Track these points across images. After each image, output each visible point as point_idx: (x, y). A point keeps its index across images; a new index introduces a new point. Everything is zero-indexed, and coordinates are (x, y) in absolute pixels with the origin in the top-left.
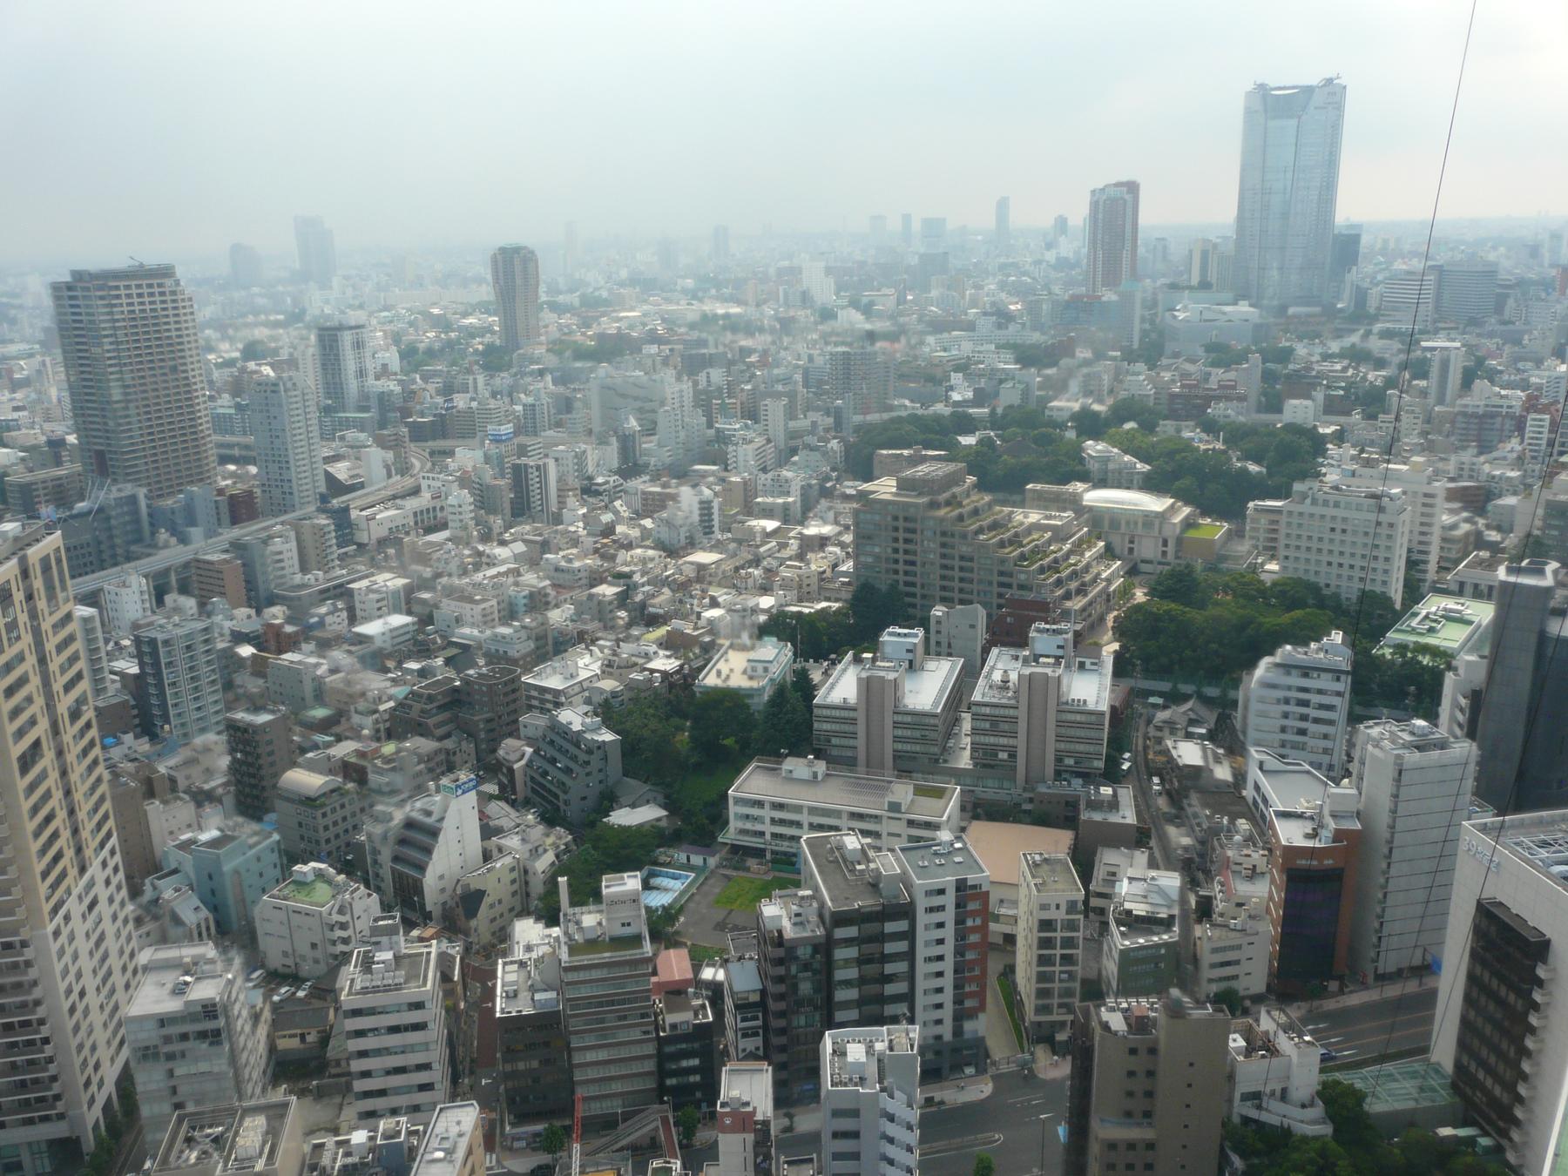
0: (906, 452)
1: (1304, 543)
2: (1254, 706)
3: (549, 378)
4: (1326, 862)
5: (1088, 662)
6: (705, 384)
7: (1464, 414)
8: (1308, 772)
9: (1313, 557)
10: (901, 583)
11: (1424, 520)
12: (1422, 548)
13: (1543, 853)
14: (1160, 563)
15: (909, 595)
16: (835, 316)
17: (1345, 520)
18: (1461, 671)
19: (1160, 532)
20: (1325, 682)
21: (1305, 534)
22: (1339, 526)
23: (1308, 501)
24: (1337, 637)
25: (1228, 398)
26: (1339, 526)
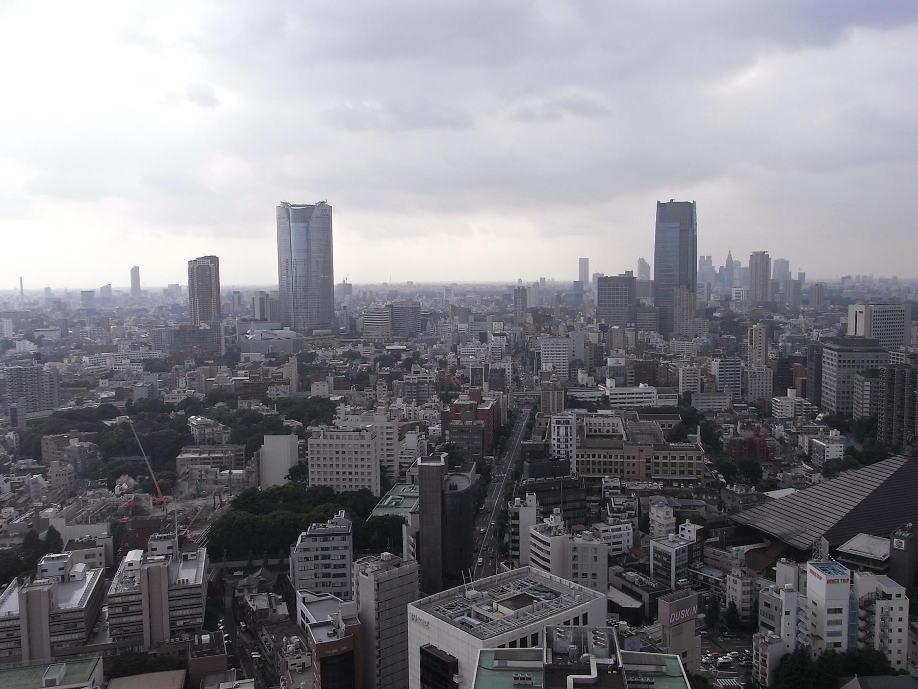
1: (322, 462)
2: (297, 564)
4: (343, 649)
5: (189, 554)
7: (408, 383)
8: (333, 598)
9: (328, 470)
13: (450, 612)
16: (14, 347)
18: (410, 523)
20: (337, 542)
21: (322, 457)
22: (340, 450)
23: (322, 437)
24: (342, 514)
25: (279, 384)
26: (340, 450)
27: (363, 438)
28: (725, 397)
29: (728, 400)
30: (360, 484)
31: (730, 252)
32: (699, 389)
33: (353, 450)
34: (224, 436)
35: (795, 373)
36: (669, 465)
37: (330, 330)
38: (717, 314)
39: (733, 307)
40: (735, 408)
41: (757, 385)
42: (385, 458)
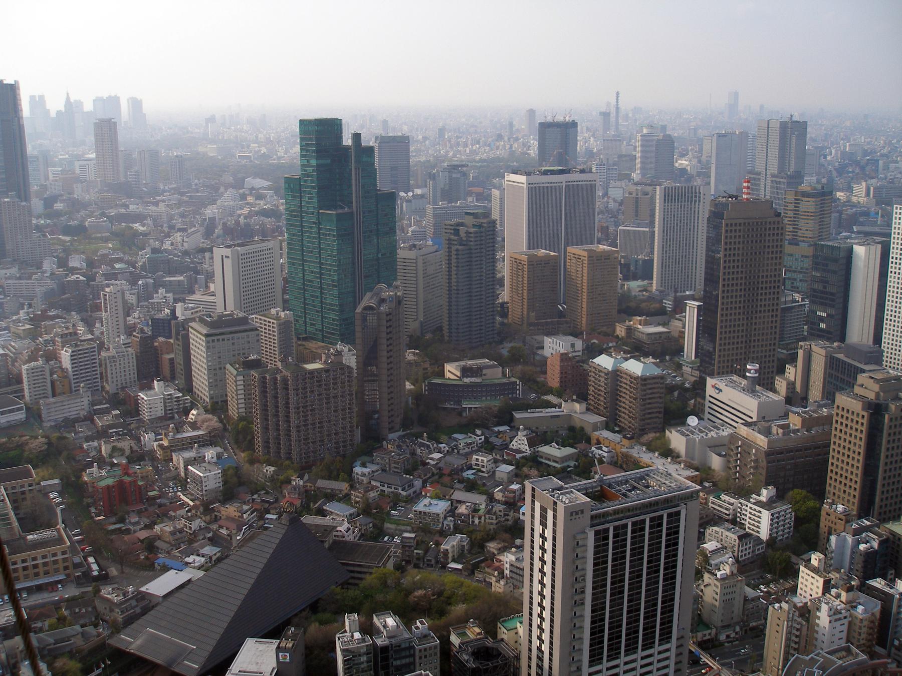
28: (82, 400)
29: (85, 401)
31: (68, 94)
32: (50, 392)
35: (161, 351)
36: (30, 568)
38: (59, 206)
39: (79, 192)
40: (97, 412)
41: (118, 371)
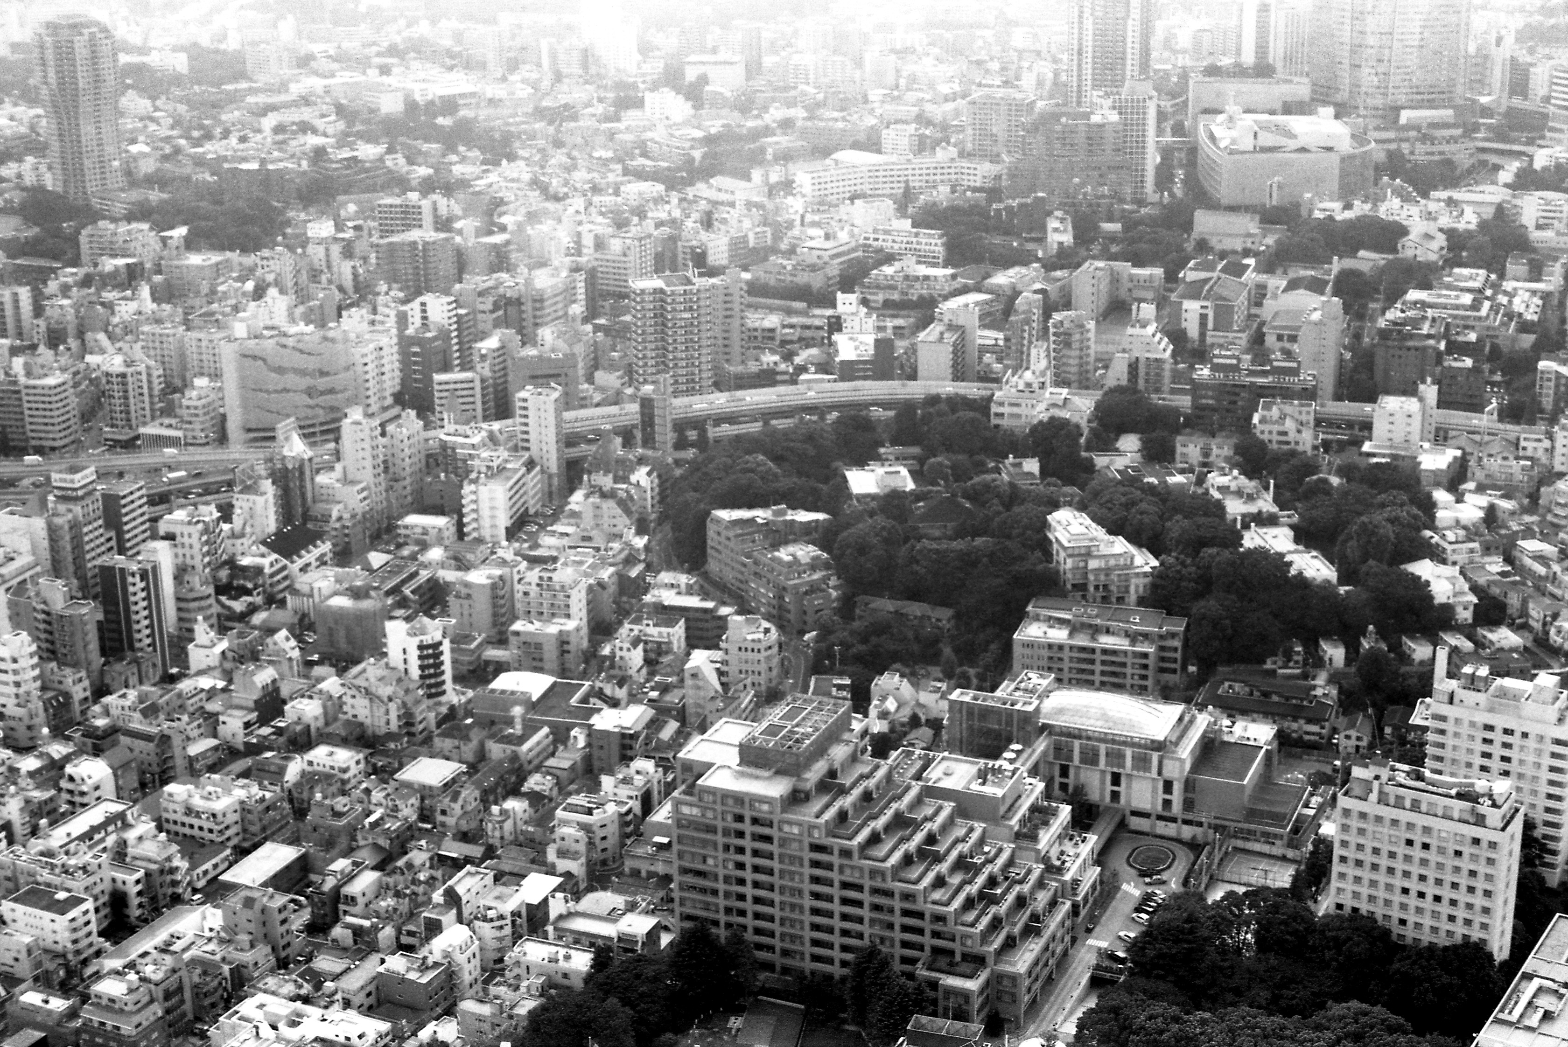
0: (761, 515)
1: (1367, 857)
3: (145, 291)
6: (418, 322)
10: (750, 930)
11: (1552, 804)
12: (1551, 817)
14: (1160, 818)
15: (760, 947)
16: (639, 104)
17: (1427, 830)
19: (1160, 773)
21: (1369, 845)
22: (1418, 839)
23: (1374, 796)
25: (1287, 394)
27: (1480, 821)
30: (1460, 930)
33: (1451, 847)
34: (1134, 581)
37: (1450, 112)
42: (1540, 816)
